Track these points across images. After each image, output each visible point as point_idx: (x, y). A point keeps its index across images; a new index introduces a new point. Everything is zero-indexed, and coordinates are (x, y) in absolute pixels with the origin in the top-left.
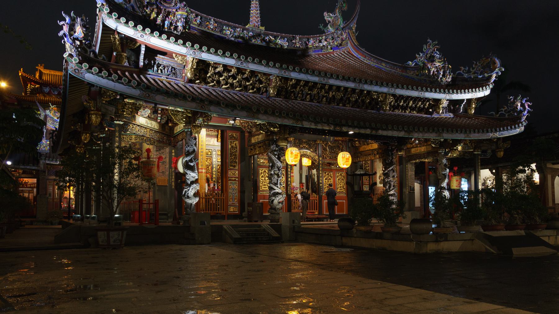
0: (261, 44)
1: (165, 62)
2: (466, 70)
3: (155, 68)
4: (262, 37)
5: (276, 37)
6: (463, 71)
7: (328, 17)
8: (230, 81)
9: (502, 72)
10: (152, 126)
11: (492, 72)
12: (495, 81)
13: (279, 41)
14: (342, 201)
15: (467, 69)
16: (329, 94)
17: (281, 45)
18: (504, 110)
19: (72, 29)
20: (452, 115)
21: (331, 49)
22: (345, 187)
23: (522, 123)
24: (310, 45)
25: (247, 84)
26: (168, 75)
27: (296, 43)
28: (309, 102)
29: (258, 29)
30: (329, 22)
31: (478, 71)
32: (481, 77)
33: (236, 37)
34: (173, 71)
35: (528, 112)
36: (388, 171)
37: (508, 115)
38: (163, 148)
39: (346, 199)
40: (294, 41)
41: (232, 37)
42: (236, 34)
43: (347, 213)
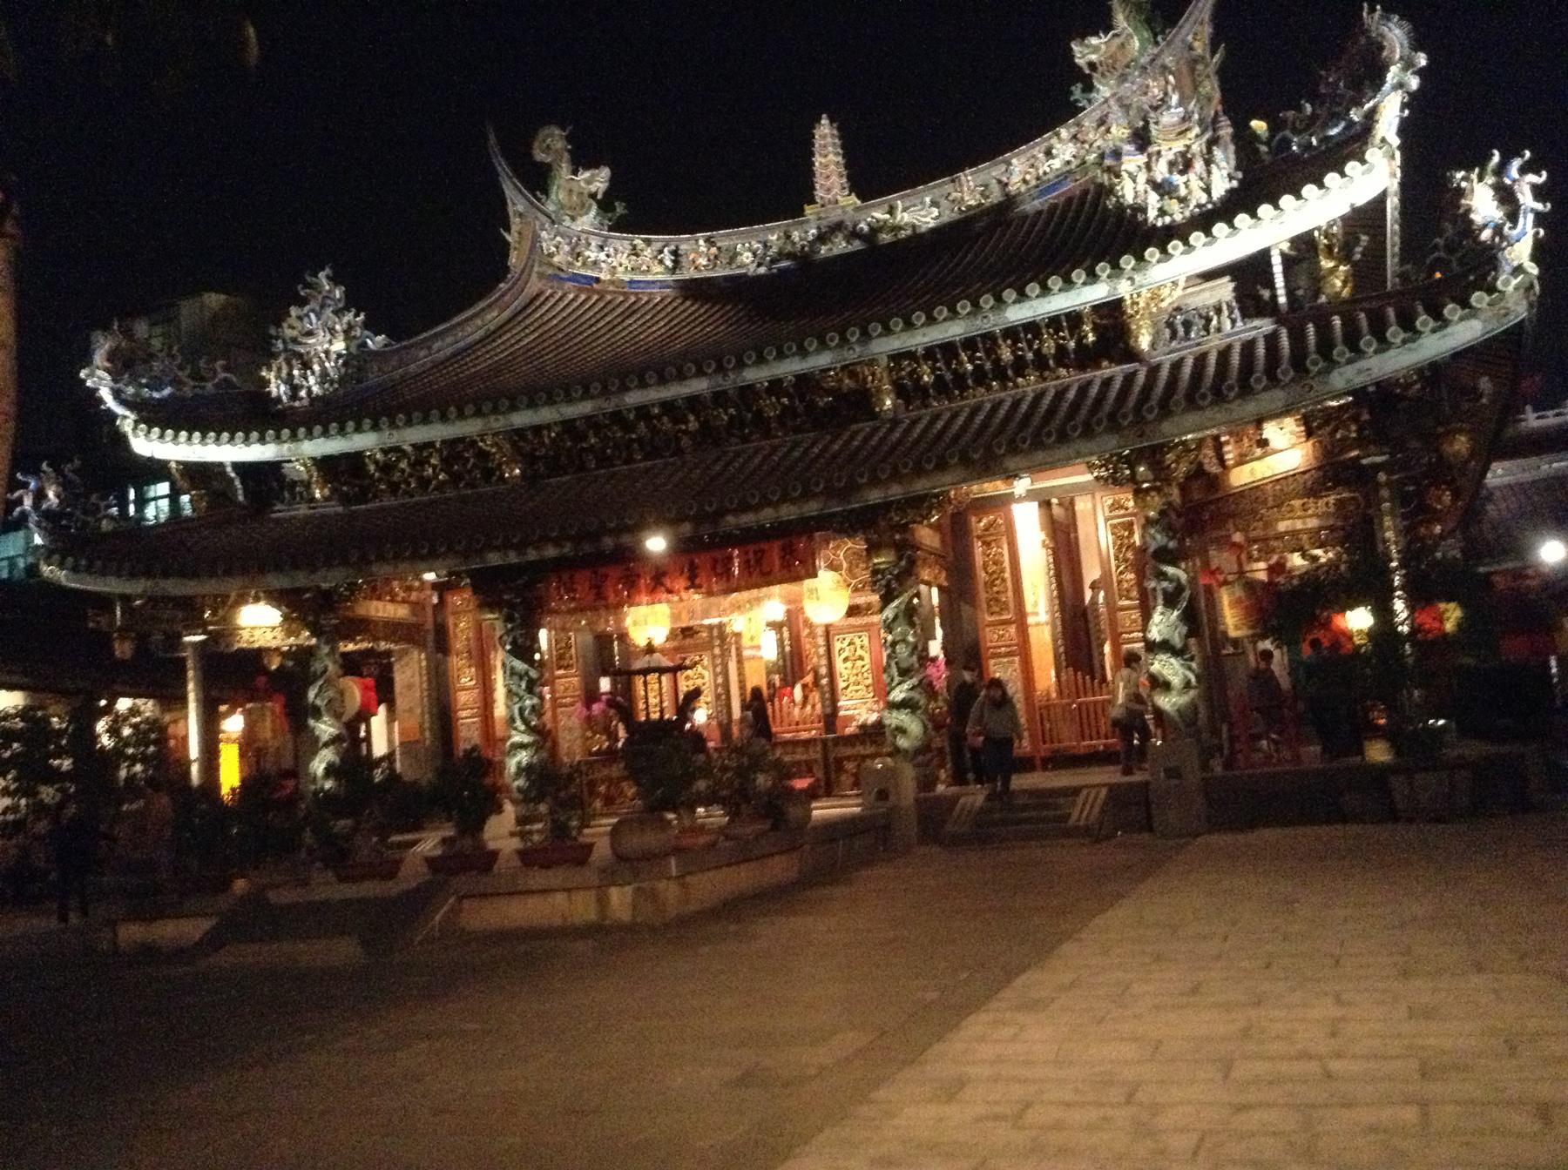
0: (850, 248)
3: (287, 495)
9: (1421, 72)
12: (1404, 129)
13: (904, 217)
16: (686, 422)
17: (914, 227)
19: (40, 496)
27: (962, 198)
28: (641, 461)
30: (1092, 65)
33: (773, 261)
35: (1540, 219)
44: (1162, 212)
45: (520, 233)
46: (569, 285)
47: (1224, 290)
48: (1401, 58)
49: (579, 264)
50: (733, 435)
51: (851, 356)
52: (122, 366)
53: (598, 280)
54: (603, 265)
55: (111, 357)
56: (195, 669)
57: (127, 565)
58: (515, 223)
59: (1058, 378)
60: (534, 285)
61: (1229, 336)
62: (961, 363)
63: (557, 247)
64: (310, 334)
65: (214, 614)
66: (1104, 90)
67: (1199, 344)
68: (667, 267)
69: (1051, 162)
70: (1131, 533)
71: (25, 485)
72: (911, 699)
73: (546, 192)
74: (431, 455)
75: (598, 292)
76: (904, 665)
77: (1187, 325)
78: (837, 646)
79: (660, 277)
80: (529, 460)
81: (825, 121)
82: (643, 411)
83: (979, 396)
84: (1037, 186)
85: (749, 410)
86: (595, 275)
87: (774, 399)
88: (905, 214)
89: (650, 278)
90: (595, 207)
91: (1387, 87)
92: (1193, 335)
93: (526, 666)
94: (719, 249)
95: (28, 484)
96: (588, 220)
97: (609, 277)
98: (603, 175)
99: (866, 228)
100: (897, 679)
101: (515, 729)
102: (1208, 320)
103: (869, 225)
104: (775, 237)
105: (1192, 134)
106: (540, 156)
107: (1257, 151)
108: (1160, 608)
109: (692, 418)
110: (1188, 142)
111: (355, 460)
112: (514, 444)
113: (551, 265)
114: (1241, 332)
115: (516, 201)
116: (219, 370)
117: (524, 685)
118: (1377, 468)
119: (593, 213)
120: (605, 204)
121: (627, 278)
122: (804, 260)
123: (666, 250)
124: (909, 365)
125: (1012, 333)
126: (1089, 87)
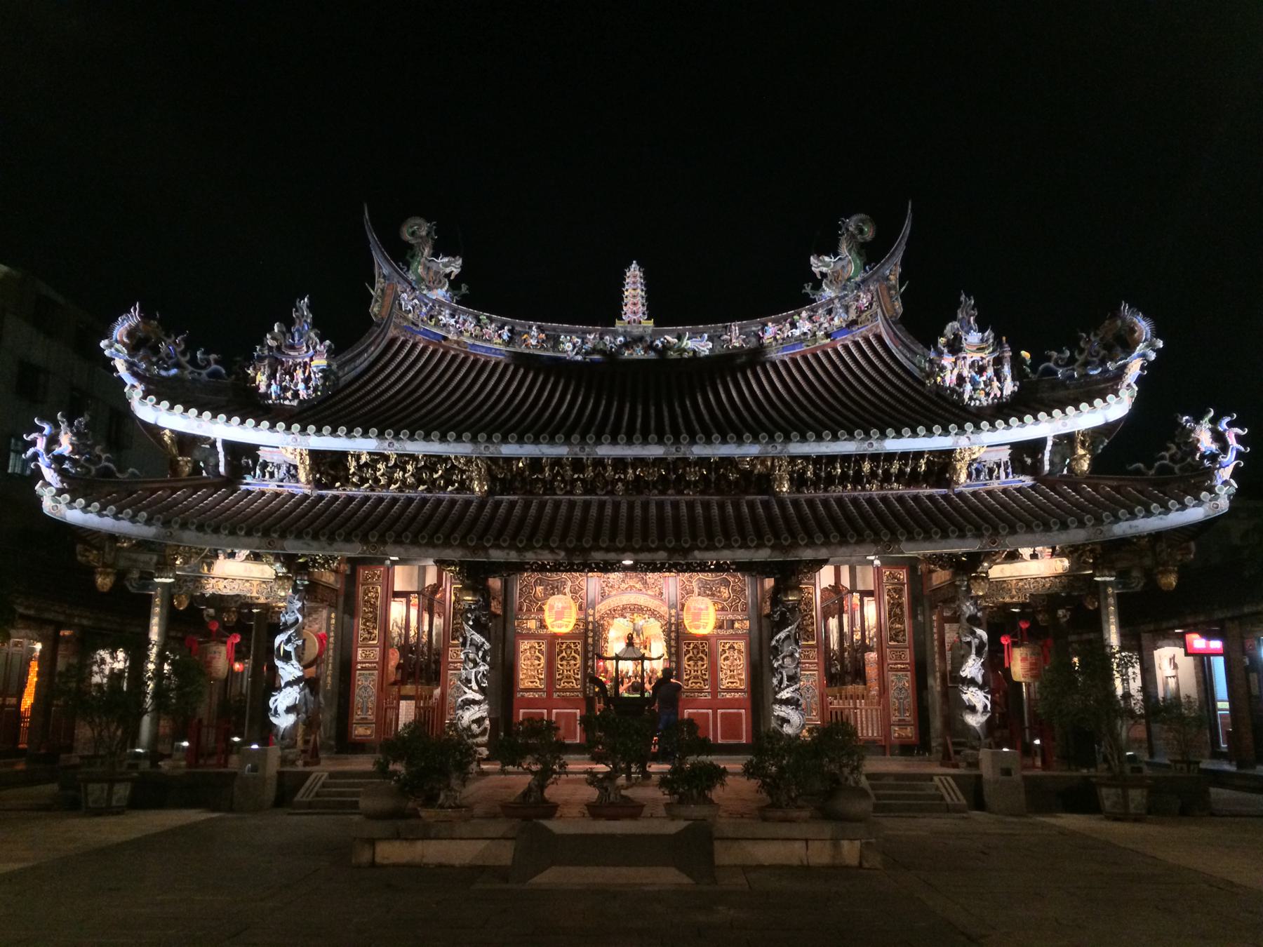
0: (646, 356)
1: (275, 458)
2: (1062, 359)
3: (258, 472)
4: (646, 341)
5: (680, 338)
6: (1057, 364)
7: (819, 265)
8: (398, 474)
9: (1158, 351)
10: (263, 574)
11: (1129, 354)
12: (1140, 381)
13: (688, 344)
15: (1068, 353)
16: (625, 473)
17: (694, 351)
18: (1167, 455)
19: (53, 441)
20: (1027, 481)
21: (828, 335)
22: (743, 677)
23: (1211, 490)
24: (767, 338)
25: (435, 476)
26: (282, 480)
27: (731, 340)
28: (581, 495)
29: (638, 328)
30: (824, 275)
31: (1093, 356)
32: (1095, 372)
33: (587, 353)
34: (293, 472)
35: (1240, 455)
36: (777, 641)
37: (1180, 469)
38: (315, 610)
39: (748, 704)
40: (725, 337)
41: (577, 354)
42: (589, 346)
43: (750, 741)
44: (971, 398)
45: (382, 290)
46: (419, 337)
47: (1004, 455)
48: (1146, 340)
49: (433, 323)
50: (656, 488)
51: (771, 450)
52: (136, 343)
53: (445, 338)
54: (451, 328)
55: (131, 333)
56: (162, 607)
57: (144, 514)
58: (380, 283)
59: (892, 489)
60: (392, 332)
61: (1004, 483)
62: (835, 468)
63: (413, 307)
64: (292, 347)
65: (185, 562)
66: (828, 292)
67: (985, 485)
68: (504, 340)
69: (794, 330)
70: (900, 597)
71: (41, 430)
72: (793, 698)
73: (408, 266)
74: (407, 462)
75: (443, 347)
76: (790, 674)
77: (978, 472)
78: (685, 648)
79: (497, 347)
80: (492, 477)
81: (634, 265)
82: (599, 463)
83: (837, 491)
84: (781, 344)
85: (675, 472)
86: (443, 333)
87: (697, 468)
88: (689, 342)
89: (488, 345)
90: (447, 284)
91: (1135, 354)
92: (982, 477)
93: (483, 640)
94: (546, 336)
95: (44, 429)
96: (440, 293)
97: (455, 338)
98: (458, 263)
99: (660, 345)
100: (785, 682)
101: (470, 688)
102: (991, 471)
103: (662, 343)
104: (592, 336)
105: (987, 352)
106: (406, 236)
107: (1024, 370)
108: (973, 656)
109: (630, 471)
110: (984, 356)
111: (339, 458)
112: (489, 469)
113: (406, 319)
114: (1010, 482)
115: (382, 266)
116: (212, 362)
117: (480, 654)
118: (1106, 584)
119: (446, 288)
120: (454, 284)
121: (470, 341)
122: (611, 357)
123: (506, 328)
124: (802, 463)
125: (875, 458)
126: (817, 286)
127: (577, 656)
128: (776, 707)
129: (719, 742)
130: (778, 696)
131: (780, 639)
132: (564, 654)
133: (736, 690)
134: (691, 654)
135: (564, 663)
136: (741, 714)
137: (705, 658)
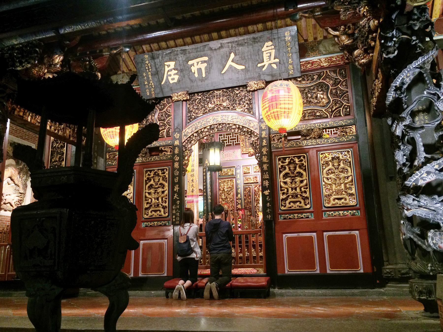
14: (295, 235)
36: (397, 89)
39: (363, 224)
43: (369, 271)
76: (430, 141)
78: (279, 164)
100: (422, 155)
127: (164, 183)
128: (409, 200)
129: (328, 272)
130: (410, 182)
131: (403, 83)
132: (152, 182)
133: (346, 208)
134: (287, 170)
135: (152, 191)
136: (354, 236)
137: (304, 173)
